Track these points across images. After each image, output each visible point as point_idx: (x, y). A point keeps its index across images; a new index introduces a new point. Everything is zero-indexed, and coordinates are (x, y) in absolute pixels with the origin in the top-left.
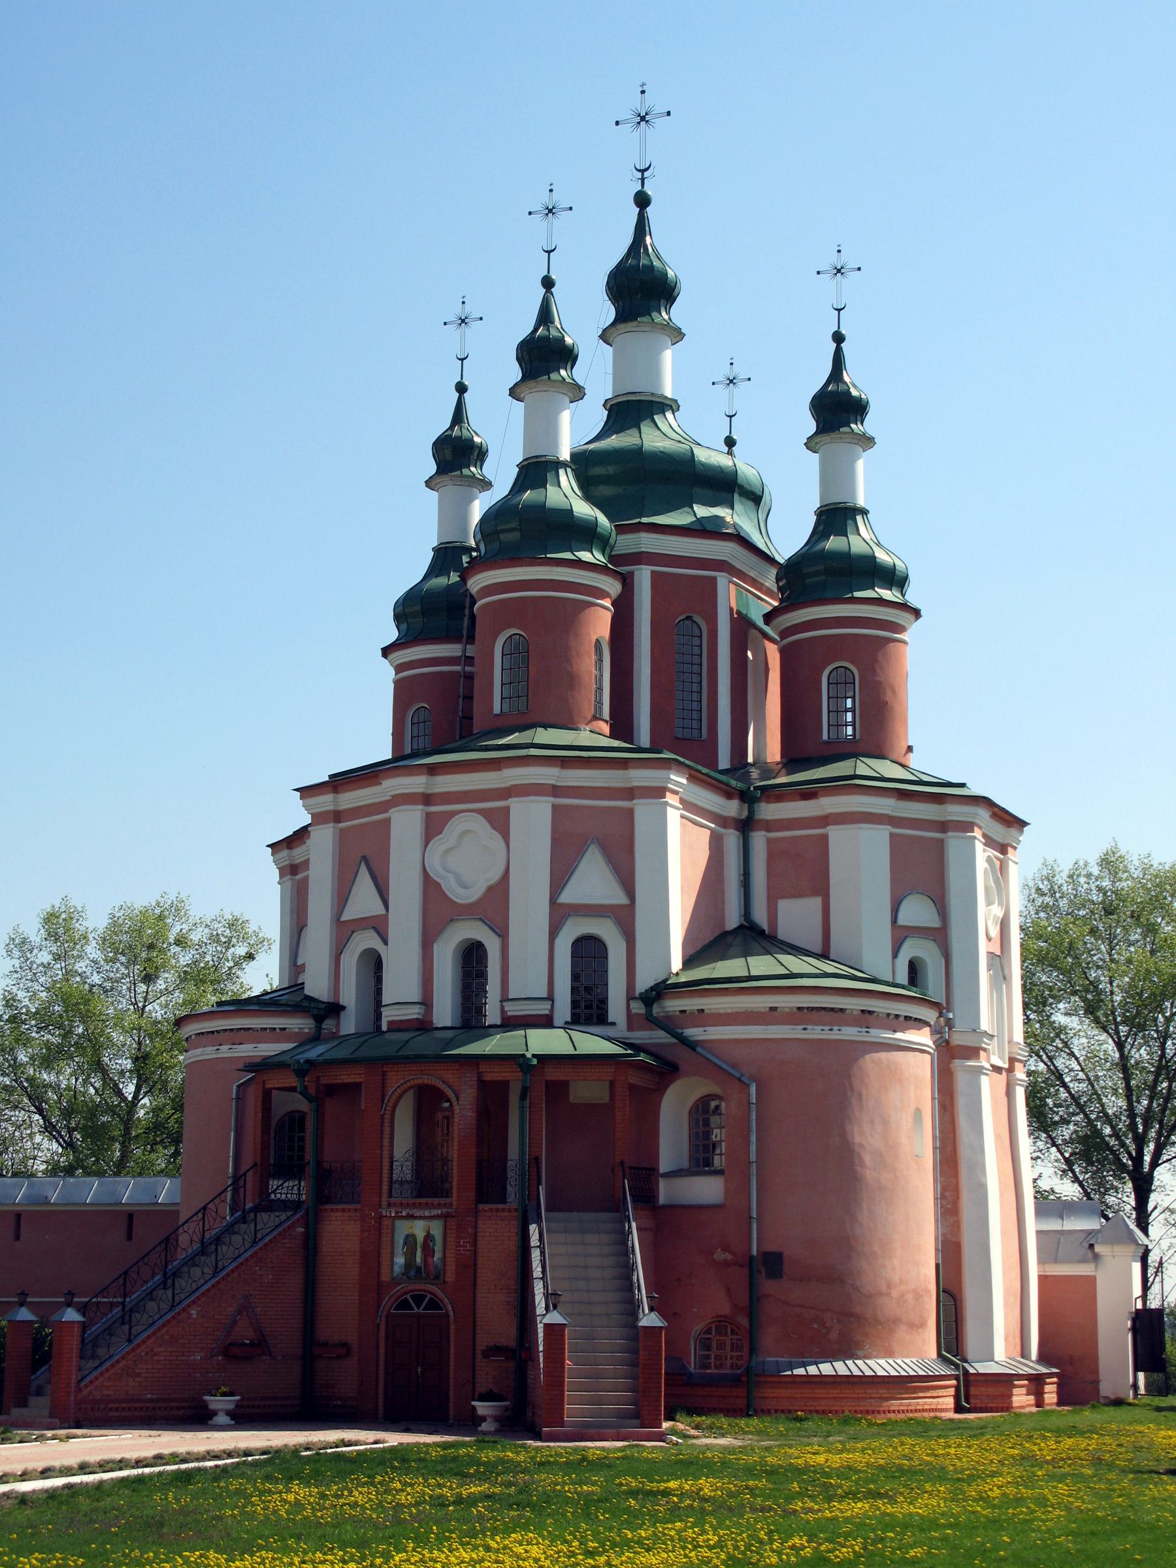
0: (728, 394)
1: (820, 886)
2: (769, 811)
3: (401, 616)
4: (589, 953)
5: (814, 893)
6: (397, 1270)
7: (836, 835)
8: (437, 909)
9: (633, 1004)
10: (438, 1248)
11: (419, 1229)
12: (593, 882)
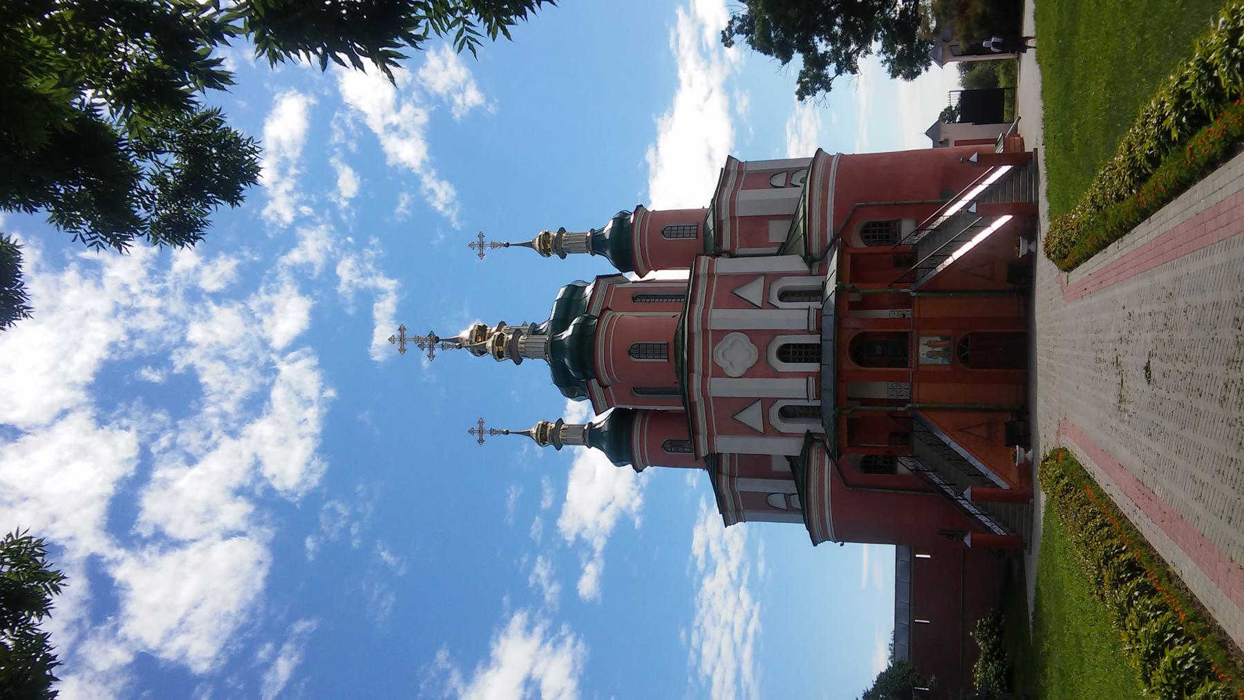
0: (535, 293)
4: (785, 295)
6: (946, 362)
7: (740, 212)
8: (760, 369)
10: (934, 339)
11: (924, 350)
12: (753, 293)
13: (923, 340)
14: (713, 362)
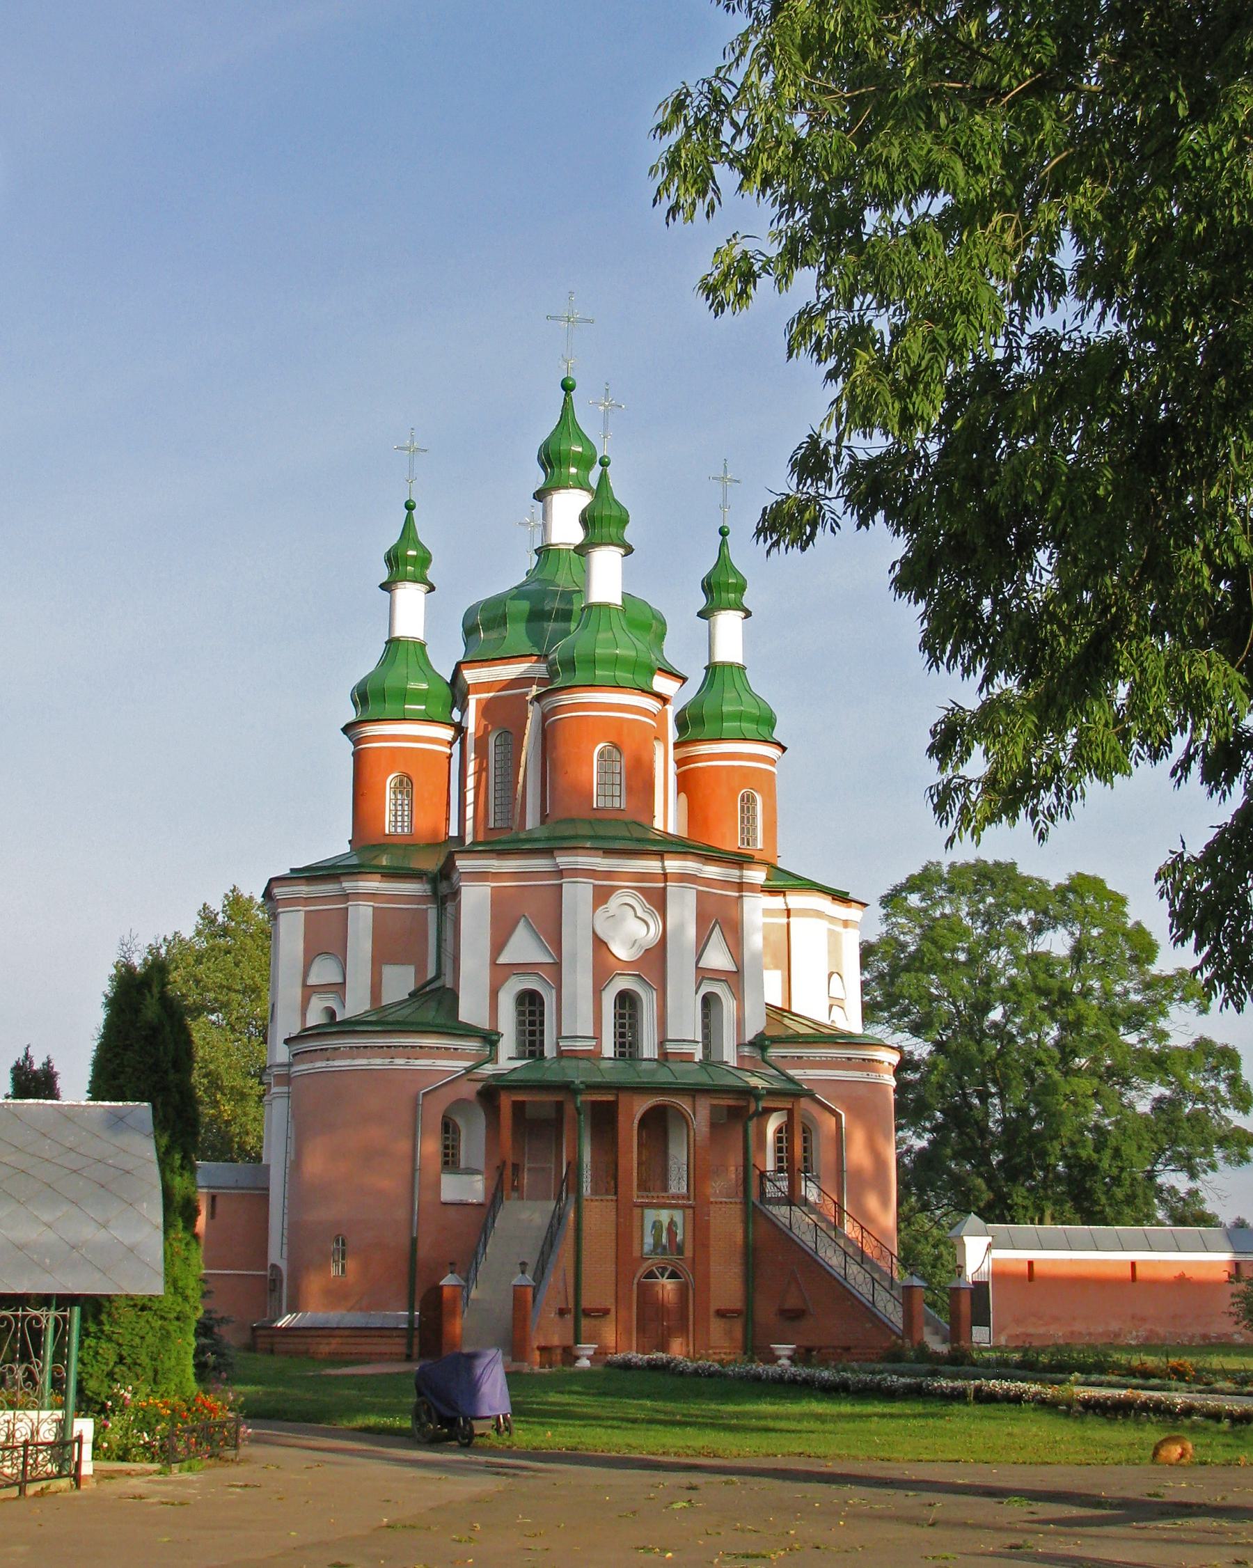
6: (647, 1248)
11: (664, 1216)
13: (678, 1216)
14: (614, 889)
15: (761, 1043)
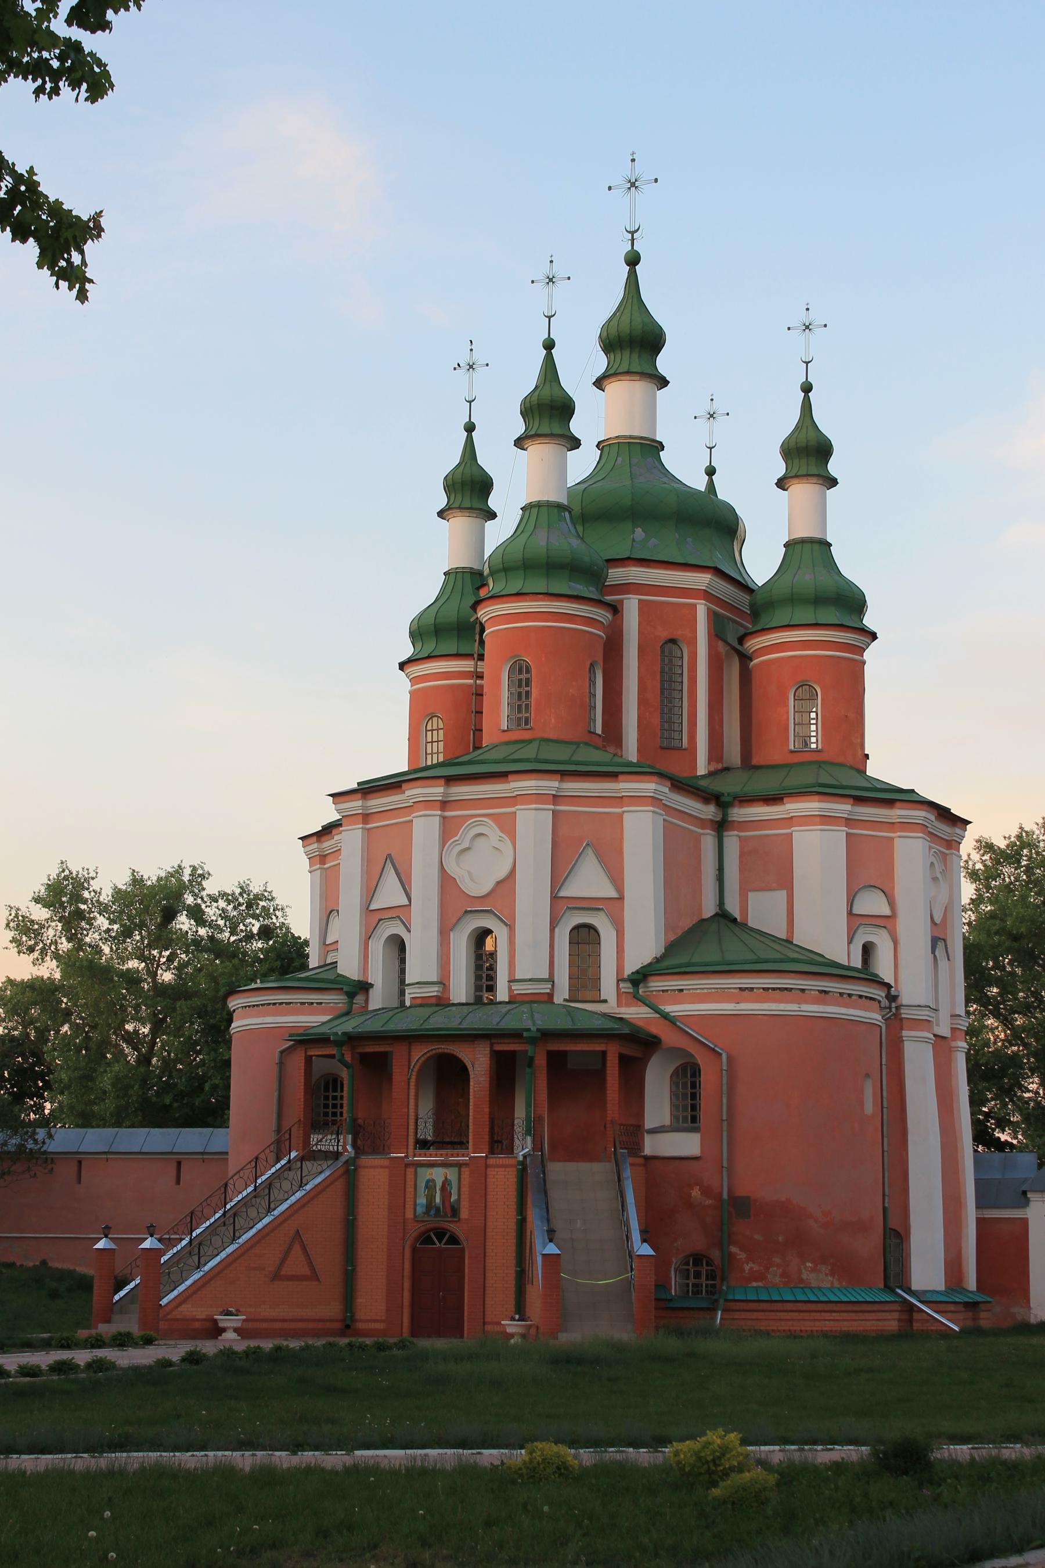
1: (785, 880)
2: (740, 813)
3: (417, 634)
5: (780, 887)
6: (420, 1210)
9: (621, 985)
11: (438, 1175)
13: (452, 1174)
15: (640, 978)
